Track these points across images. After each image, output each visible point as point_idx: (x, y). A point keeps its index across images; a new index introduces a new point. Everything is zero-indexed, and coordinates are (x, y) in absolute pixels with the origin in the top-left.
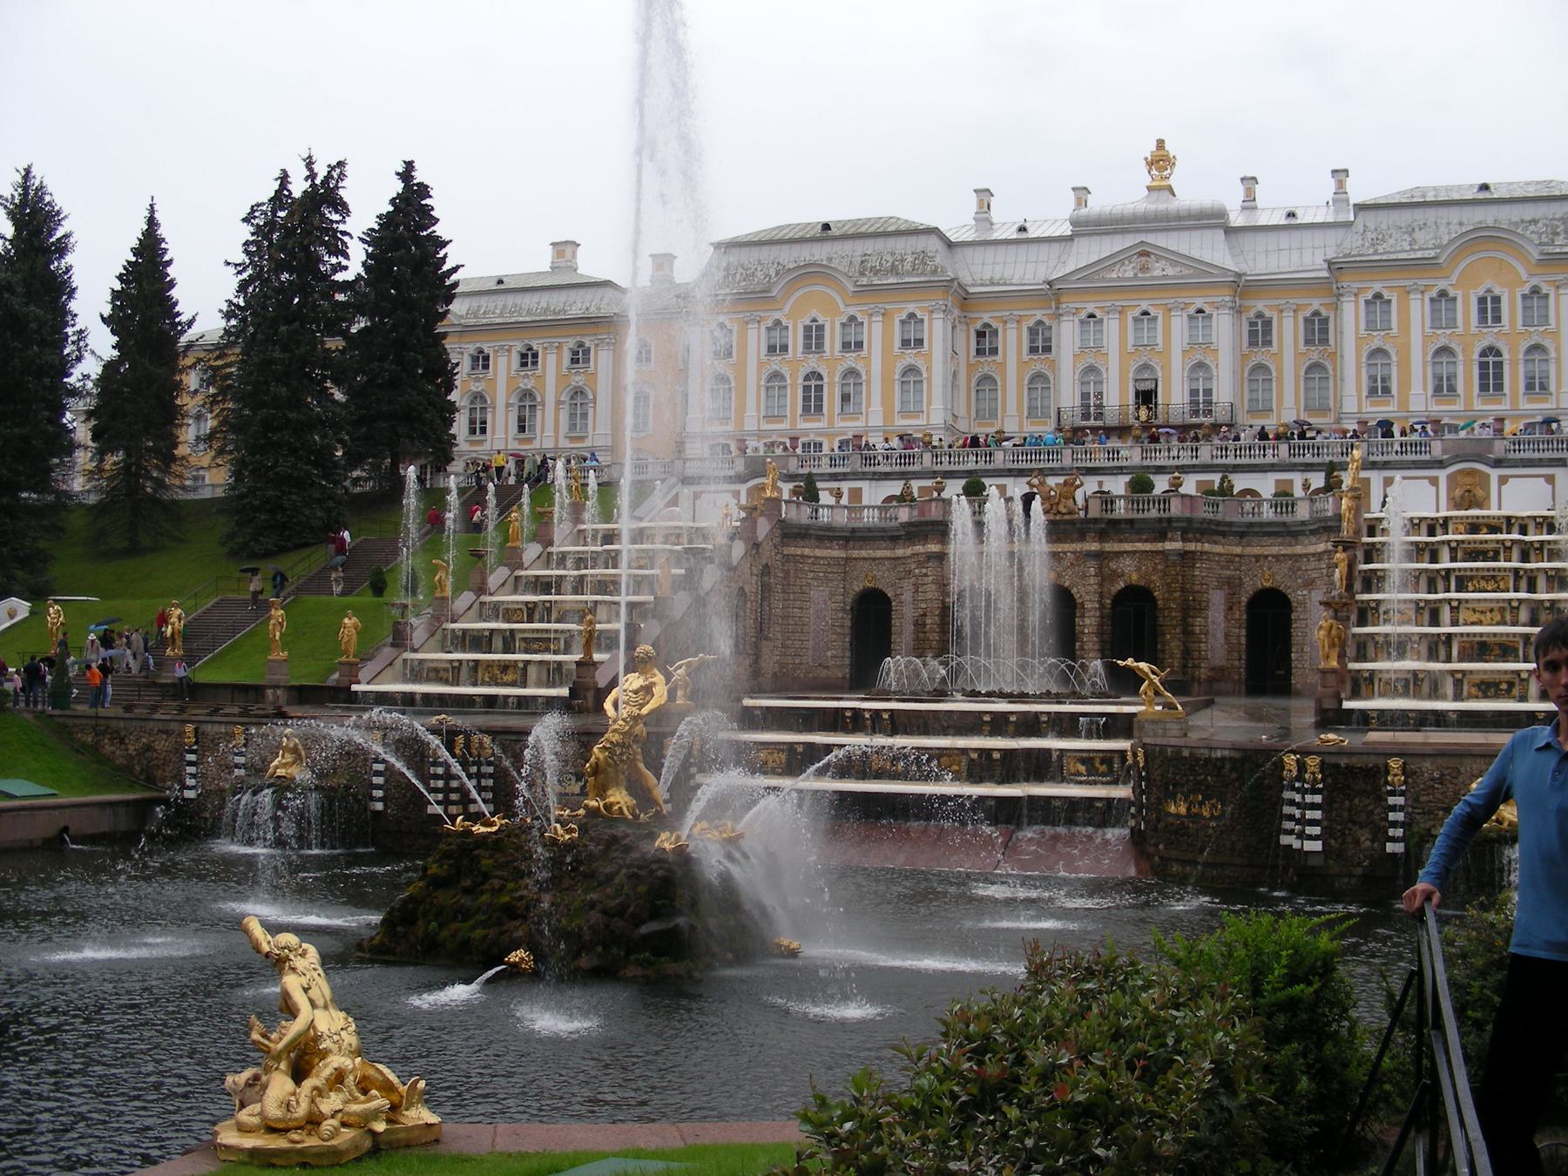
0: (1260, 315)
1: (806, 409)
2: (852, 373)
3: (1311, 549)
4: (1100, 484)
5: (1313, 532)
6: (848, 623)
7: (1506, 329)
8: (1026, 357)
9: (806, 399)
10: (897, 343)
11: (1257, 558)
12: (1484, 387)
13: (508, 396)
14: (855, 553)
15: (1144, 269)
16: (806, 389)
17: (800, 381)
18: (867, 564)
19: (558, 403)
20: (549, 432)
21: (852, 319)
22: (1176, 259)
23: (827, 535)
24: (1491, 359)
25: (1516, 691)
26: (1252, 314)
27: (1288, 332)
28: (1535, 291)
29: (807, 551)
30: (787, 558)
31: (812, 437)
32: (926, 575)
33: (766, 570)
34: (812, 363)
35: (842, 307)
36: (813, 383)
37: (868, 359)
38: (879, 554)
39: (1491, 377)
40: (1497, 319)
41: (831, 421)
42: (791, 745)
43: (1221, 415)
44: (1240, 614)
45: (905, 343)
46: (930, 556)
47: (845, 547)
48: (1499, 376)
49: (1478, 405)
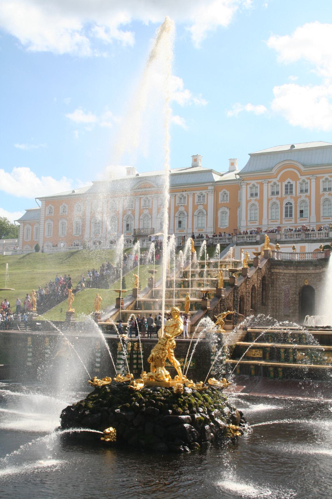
1: (286, 216)
2: (303, 201)
6: (297, 299)
9: (286, 212)
10: (321, 190)
13: (175, 214)
14: (300, 272)
16: (286, 208)
17: (284, 205)
19: (193, 215)
20: (190, 226)
21: (304, 181)
23: (288, 264)
29: (281, 271)
30: (272, 274)
31: (288, 227)
33: (264, 278)
34: (289, 199)
35: (300, 177)
36: (289, 206)
37: (310, 197)
41: (296, 223)
45: (325, 190)
47: (296, 269)
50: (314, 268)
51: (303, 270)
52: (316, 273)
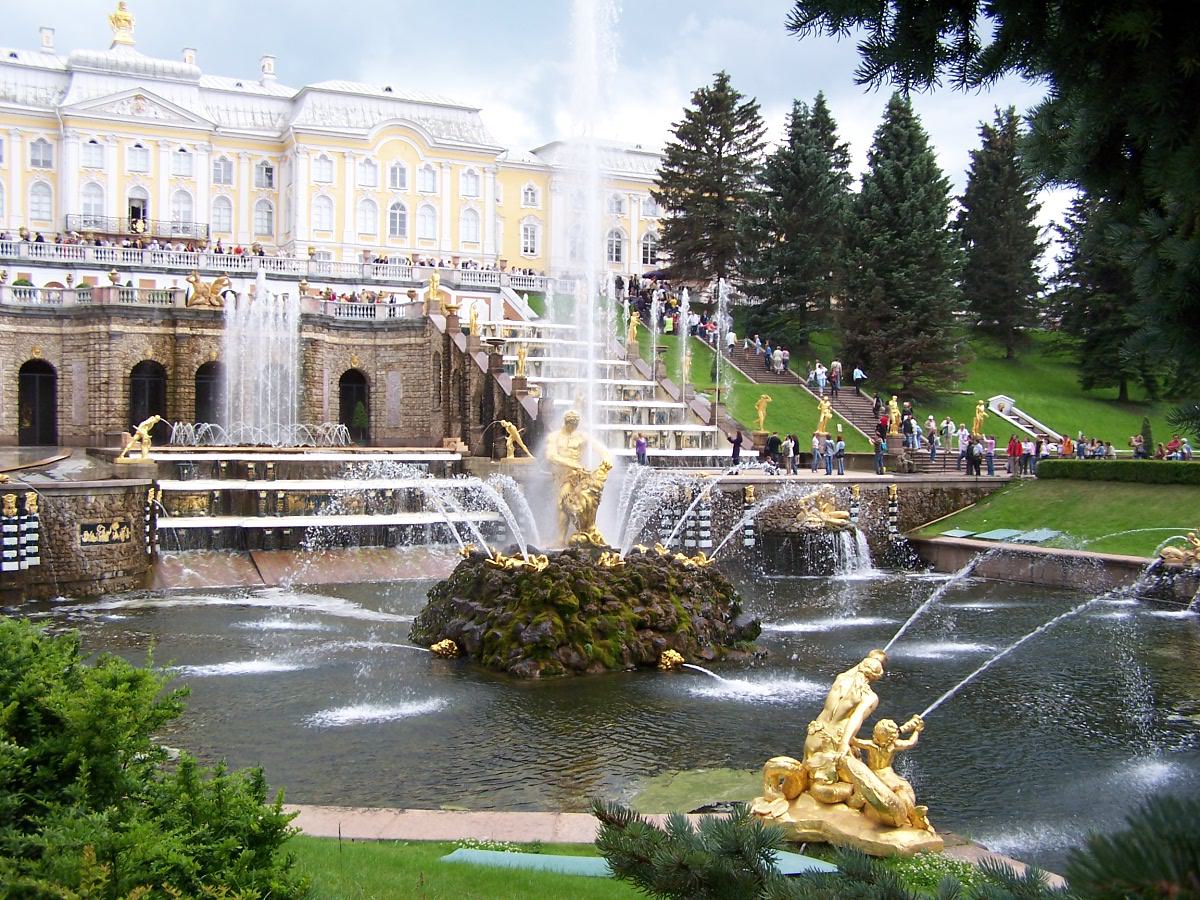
0: (223, 159)
3: (390, 342)
4: (175, 282)
5: (390, 330)
6: (17, 388)
7: (409, 192)
8: (30, 168)
11: (348, 347)
12: (393, 231)
14: (24, 328)
15: (139, 110)
18: (33, 338)
22: (168, 106)
24: (398, 212)
25: (658, 443)
26: (217, 157)
27: (246, 175)
28: (428, 168)
32: (108, 350)
38: (46, 330)
39: (398, 222)
40: (403, 184)
42: (212, 492)
43: (202, 236)
44: (337, 388)
46: (111, 336)
48: (403, 224)
49: (389, 243)
50: (58, 323)
51: (28, 324)
52: (61, 334)
